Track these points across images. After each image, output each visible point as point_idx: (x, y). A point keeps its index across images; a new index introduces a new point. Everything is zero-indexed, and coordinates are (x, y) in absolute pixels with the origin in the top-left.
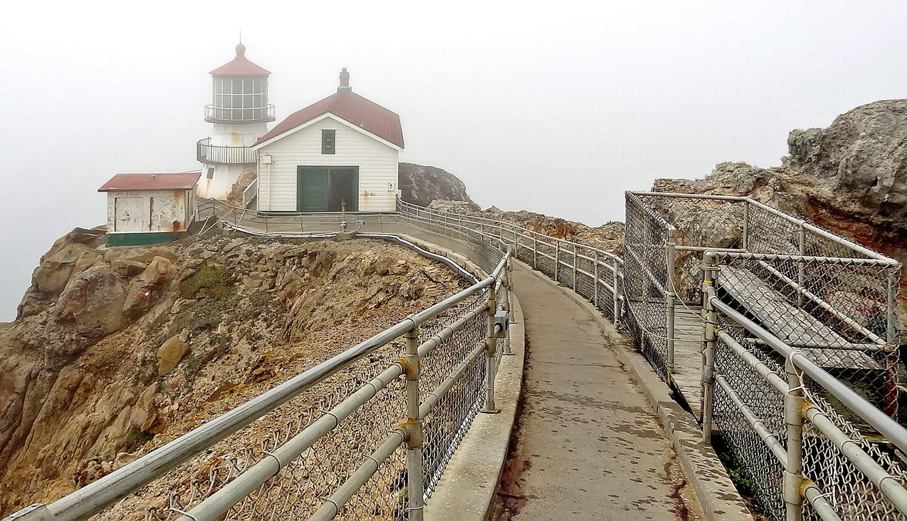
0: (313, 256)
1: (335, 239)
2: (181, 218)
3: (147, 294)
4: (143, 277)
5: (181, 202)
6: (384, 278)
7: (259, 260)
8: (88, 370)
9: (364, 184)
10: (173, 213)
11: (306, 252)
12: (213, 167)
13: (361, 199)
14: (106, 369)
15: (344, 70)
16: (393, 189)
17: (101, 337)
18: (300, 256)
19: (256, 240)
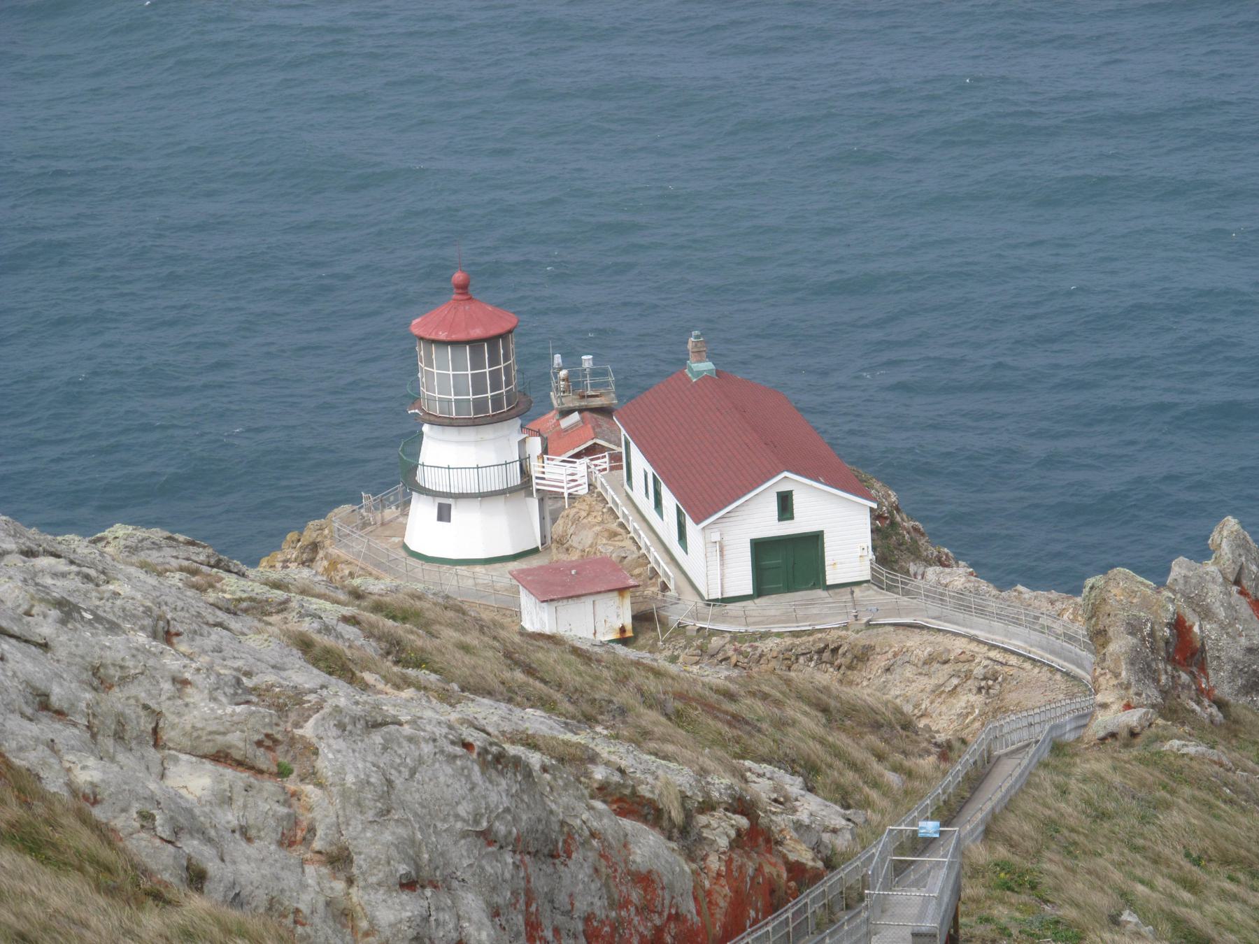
0: (835, 651)
1: (846, 627)
2: (628, 622)
5: (627, 602)
6: (946, 666)
11: (827, 646)
12: (450, 501)
16: (865, 553)
18: (820, 652)
19: (735, 637)
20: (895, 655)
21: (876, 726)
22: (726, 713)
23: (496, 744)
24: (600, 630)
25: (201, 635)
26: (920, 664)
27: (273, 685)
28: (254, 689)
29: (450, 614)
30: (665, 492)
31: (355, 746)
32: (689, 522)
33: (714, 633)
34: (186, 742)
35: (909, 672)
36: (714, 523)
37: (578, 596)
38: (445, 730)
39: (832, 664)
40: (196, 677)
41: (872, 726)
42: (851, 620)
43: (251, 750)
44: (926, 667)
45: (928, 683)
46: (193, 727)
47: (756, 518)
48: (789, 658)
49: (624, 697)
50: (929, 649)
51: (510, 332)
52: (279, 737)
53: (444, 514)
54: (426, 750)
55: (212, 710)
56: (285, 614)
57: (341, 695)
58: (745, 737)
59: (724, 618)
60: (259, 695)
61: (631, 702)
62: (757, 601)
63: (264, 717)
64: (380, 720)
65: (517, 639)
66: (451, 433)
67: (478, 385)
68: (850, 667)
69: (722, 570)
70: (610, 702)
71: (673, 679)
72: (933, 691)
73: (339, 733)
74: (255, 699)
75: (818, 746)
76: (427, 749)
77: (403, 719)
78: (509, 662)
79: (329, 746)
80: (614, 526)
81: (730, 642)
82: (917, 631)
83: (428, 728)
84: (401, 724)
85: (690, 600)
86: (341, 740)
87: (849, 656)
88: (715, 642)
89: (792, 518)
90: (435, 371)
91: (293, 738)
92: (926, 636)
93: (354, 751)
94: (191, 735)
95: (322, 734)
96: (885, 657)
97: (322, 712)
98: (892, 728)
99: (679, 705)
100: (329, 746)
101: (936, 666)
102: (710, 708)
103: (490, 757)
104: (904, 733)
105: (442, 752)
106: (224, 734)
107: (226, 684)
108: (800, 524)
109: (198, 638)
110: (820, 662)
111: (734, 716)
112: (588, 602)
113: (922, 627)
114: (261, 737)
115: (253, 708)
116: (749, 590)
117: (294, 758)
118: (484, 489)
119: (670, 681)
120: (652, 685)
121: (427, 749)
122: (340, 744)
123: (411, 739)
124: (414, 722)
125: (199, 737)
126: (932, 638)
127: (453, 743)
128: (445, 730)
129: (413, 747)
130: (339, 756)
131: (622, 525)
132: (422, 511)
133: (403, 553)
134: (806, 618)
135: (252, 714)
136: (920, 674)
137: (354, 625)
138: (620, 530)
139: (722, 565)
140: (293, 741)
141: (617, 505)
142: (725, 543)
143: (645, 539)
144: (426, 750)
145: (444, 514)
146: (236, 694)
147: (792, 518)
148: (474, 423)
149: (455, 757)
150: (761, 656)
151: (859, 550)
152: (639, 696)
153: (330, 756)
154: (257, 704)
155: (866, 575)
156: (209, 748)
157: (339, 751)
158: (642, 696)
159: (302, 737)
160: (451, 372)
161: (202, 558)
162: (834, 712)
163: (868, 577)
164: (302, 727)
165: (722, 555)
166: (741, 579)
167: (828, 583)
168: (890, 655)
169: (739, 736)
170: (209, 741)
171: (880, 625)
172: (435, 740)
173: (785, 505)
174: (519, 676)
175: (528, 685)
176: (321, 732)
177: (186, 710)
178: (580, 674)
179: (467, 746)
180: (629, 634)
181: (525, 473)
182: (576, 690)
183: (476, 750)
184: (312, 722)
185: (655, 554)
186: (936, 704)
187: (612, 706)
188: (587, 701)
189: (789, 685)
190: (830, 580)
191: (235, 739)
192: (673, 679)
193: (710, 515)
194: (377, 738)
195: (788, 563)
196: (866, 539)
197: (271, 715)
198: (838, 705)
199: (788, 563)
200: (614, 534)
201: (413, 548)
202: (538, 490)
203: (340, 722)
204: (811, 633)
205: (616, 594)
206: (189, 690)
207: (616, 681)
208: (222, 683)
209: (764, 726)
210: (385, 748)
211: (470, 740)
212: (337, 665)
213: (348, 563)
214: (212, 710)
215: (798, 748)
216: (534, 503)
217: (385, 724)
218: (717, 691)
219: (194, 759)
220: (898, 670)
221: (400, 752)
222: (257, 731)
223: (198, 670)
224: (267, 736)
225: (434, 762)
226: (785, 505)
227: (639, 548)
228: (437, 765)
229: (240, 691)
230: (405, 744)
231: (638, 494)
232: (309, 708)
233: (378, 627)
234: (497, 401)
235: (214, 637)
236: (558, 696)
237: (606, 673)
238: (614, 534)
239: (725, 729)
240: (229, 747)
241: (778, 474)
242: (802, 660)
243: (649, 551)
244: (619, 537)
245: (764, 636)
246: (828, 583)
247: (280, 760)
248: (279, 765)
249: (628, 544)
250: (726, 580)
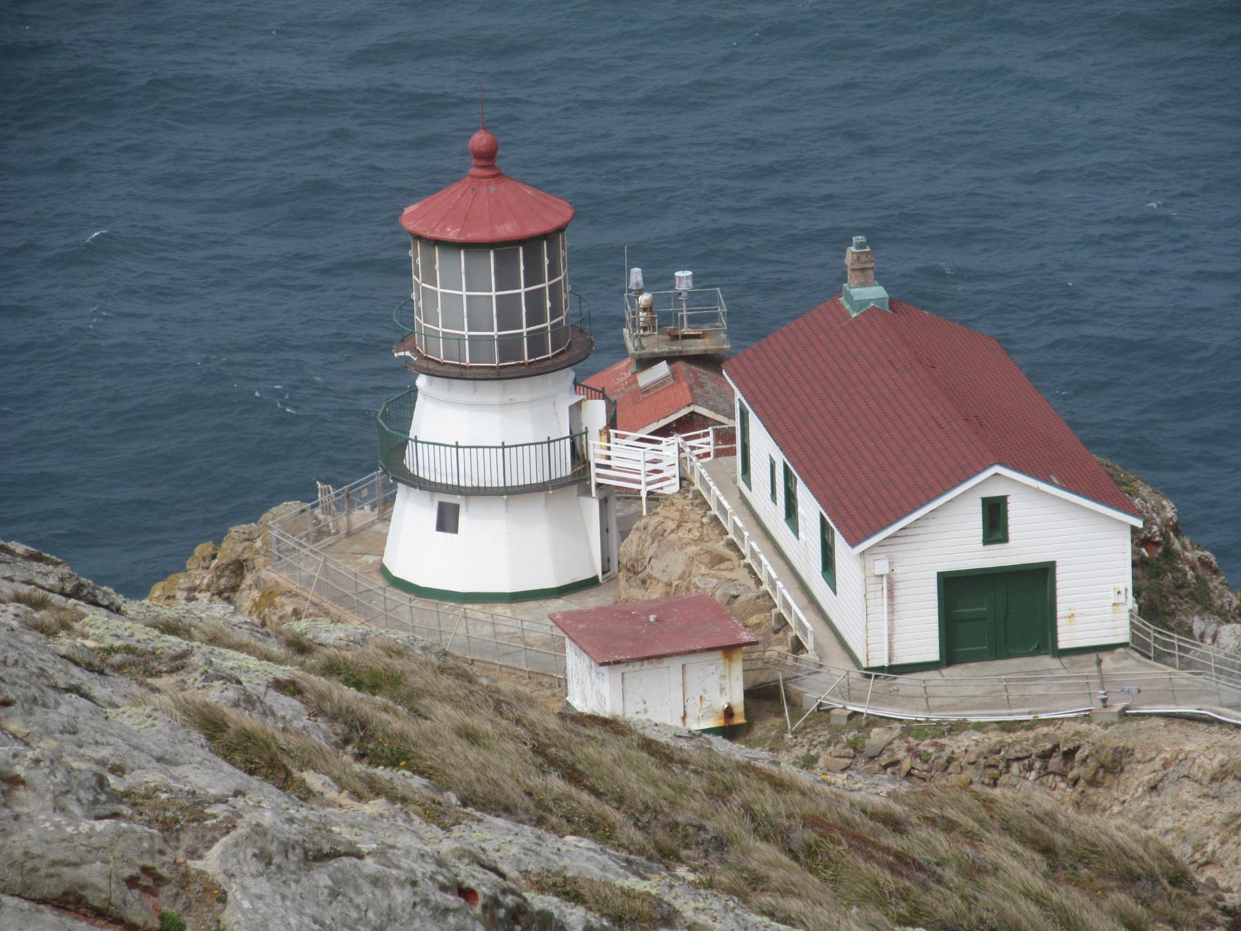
0: (1069, 755)
1: (1087, 718)
2: (736, 698)
5: (738, 668)
7: (946, 769)
10: (722, 690)
11: (1056, 747)
16: (1122, 599)
18: (1046, 756)
19: (909, 729)
20: (1166, 765)
21: (1129, 879)
22: (887, 850)
23: (513, 892)
24: (694, 711)
25: (44, 705)
26: (1206, 780)
27: (156, 789)
28: (127, 794)
29: (446, 681)
30: (803, 494)
31: (287, 891)
32: (839, 542)
33: (874, 721)
34: (14, 877)
35: (1188, 792)
36: (879, 545)
37: (660, 657)
38: (431, 868)
39: (1063, 775)
40: (33, 773)
41: (1123, 879)
42: (1096, 706)
43: (118, 893)
44: (1216, 785)
45: (1218, 811)
46: (26, 853)
47: (949, 538)
48: (995, 766)
49: (725, 821)
50: (1220, 757)
51: (561, 229)
52: (164, 872)
53: (447, 521)
54: (400, 899)
55: (57, 826)
56: (182, 675)
57: (266, 807)
58: (917, 890)
59: (890, 698)
60: (134, 805)
61: (736, 829)
62: (947, 672)
63: (140, 839)
64: (326, 848)
65: (553, 724)
66: (462, 391)
67: (508, 316)
68: (1093, 782)
69: (891, 621)
70: (701, 828)
71: (803, 794)
72: (1227, 824)
73: (261, 867)
74: (126, 810)
75: (1034, 909)
76: (401, 896)
77: (364, 847)
78: (540, 760)
79: (244, 888)
80: (720, 547)
81: (901, 737)
82: (1202, 726)
83: (404, 863)
84: (360, 856)
85: (838, 667)
86: (263, 879)
87: (1092, 763)
88: (878, 736)
89: (1005, 539)
90: (439, 290)
91: (186, 875)
92: (1217, 735)
93: (284, 897)
94: (22, 865)
95: (233, 870)
96: (1150, 767)
97: (233, 833)
98: (1154, 880)
99: (811, 835)
100: (244, 888)
102: (860, 843)
103: (502, 913)
104: (1175, 891)
105: (426, 902)
106: (76, 865)
107: (80, 784)
108: (1018, 551)
109: (38, 710)
110: (1045, 771)
111: (899, 856)
112: (675, 665)
113: (1210, 721)
114: (135, 871)
115: (124, 825)
116: (932, 653)
117: (187, 907)
118: (513, 481)
119: (798, 797)
120: (768, 802)
121: (401, 896)
122: (262, 886)
123: (375, 881)
124: (382, 853)
125: (35, 870)
126: (1226, 739)
127: (443, 888)
128: (431, 868)
129: (378, 892)
130: (260, 904)
131: (732, 545)
132: (412, 515)
133: (380, 581)
134: (1024, 701)
135: (121, 834)
136: (1206, 796)
137: (293, 695)
138: (728, 552)
139: (892, 612)
140: (186, 879)
141: (724, 512)
142: (897, 578)
143: (768, 568)
144: (400, 899)
145: (447, 521)
146: (96, 802)
147: (1005, 539)
148: (499, 375)
149: (447, 911)
150: (950, 760)
151: (1112, 594)
152: (747, 820)
153: (246, 904)
154: (129, 819)
155: (1123, 635)
156: (50, 888)
157: (260, 897)
158: (753, 820)
159: (201, 873)
160: (464, 293)
161: (52, 581)
162: (1062, 853)
163: (1123, 635)
164: (200, 857)
165: (891, 596)
166: (921, 638)
167: (1062, 644)
168: (1157, 764)
169: (908, 889)
170: (51, 876)
171: (1143, 715)
172: (414, 883)
173: (995, 520)
174: (556, 783)
175: (570, 797)
176: (231, 865)
177: (16, 825)
178: (654, 783)
179: (467, 894)
180: (739, 719)
181: (579, 457)
182: (647, 808)
183: (481, 901)
184: (217, 849)
185: (784, 593)
186: (1230, 846)
187: (703, 835)
188: (663, 827)
189: (989, 809)
190: (1065, 640)
191: (93, 873)
192: (803, 794)
193: (875, 532)
194: (322, 877)
195: (997, 612)
196: (1125, 578)
197: (152, 837)
198: (1068, 842)
199: (997, 612)
200: (718, 560)
201: (397, 572)
202: (599, 485)
203: (262, 850)
204: (1030, 725)
205: (719, 655)
206: (21, 793)
207: (710, 794)
208: (74, 783)
209: (949, 873)
210: (334, 894)
211: (472, 883)
212: (261, 758)
213: (290, 594)
214: (57, 826)
215: (1002, 911)
216: (592, 506)
217: (334, 855)
218: (874, 816)
219: (26, 905)
220: (1171, 789)
221: (358, 900)
222: (130, 863)
223: (37, 761)
224: (145, 870)
225: (412, 918)
226: (995, 520)
227: (759, 582)
228: (417, 923)
229: (103, 798)
230: (366, 887)
231: (759, 496)
232: (214, 828)
233: (331, 700)
234: (536, 341)
235: (64, 709)
236: (616, 816)
237: (695, 782)
238: (721, 559)
239: (886, 877)
240: (83, 887)
241: (985, 468)
242: (1015, 768)
243: (774, 588)
244: (726, 565)
245: (956, 728)
246: (1062, 644)
247: (165, 908)
248: (162, 918)
249: (742, 575)
250: (896, 638)
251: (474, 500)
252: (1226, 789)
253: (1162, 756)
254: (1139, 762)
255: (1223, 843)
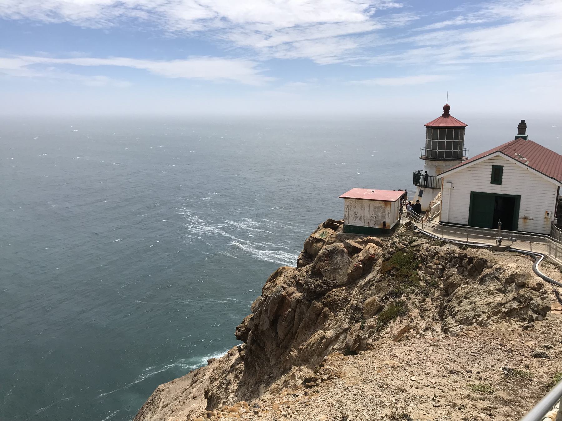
3: (361, 266)
4: (360, 254)
8: (325, 305)
9: (524, 209)
13: (520, 221)
14: (335, 306)
15: (523, 121)
17: (336, 286)
89: (500, 184)
101: (513, 286)
108: (506, 188)
116: (466, 221)
136: (500, 290)
173: (497, 175)
226: (497, 175)
251: (427, 189)
252: (509, 288)
253: (495, 266)
254: (488, 268)
255: (488, 318)
